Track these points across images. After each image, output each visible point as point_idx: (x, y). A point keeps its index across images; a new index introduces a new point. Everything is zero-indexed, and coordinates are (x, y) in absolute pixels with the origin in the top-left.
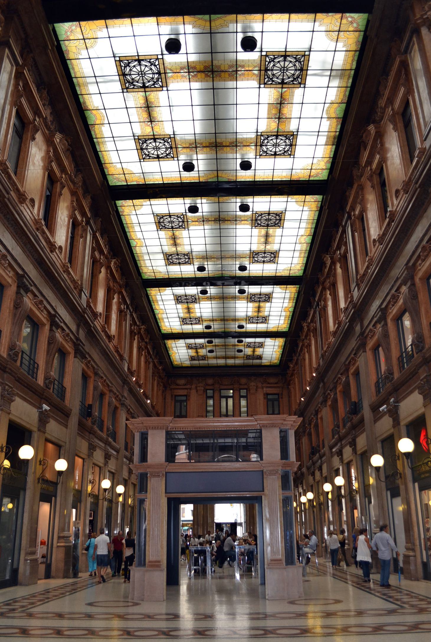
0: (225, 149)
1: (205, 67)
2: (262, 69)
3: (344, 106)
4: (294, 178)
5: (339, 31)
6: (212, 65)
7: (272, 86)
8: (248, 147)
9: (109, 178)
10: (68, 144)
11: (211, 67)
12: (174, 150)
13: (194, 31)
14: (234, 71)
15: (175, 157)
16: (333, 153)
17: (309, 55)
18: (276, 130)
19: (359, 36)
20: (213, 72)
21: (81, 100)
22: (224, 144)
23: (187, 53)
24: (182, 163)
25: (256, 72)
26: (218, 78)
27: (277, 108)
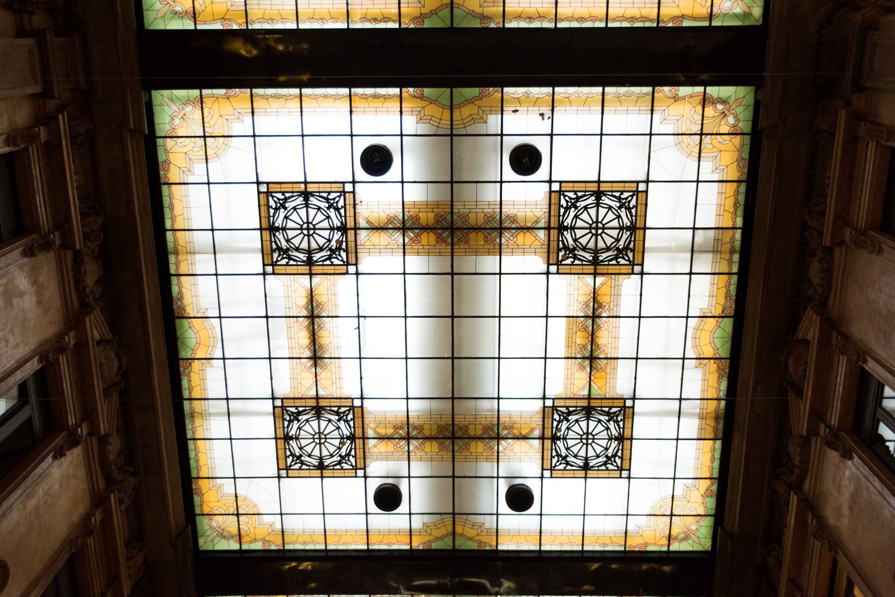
0: (473, 444)
1: (438, 218)
2: (552, 225)
3: (728, 324)
4: (634, 544)
5: (701, 134)
6: (452, 212)
7: (574, 269)
8: (523, 443)
9: (204, 524)
10: (119, 368)
11: (449, 218)
12: (359, 442)
13: (422, 129)
14: (496, 230)
15: (360, 468)
16: (716, 464)
17: (646, 192)
18: (586, 392)
19: (742, 146)
20: (453, 231)
21: (175, 290)
22: (472, 433)
23: (402, 182)
24: (374, 485)
25: (542, 234)
26: (463, 246)
27: (585, 329)
